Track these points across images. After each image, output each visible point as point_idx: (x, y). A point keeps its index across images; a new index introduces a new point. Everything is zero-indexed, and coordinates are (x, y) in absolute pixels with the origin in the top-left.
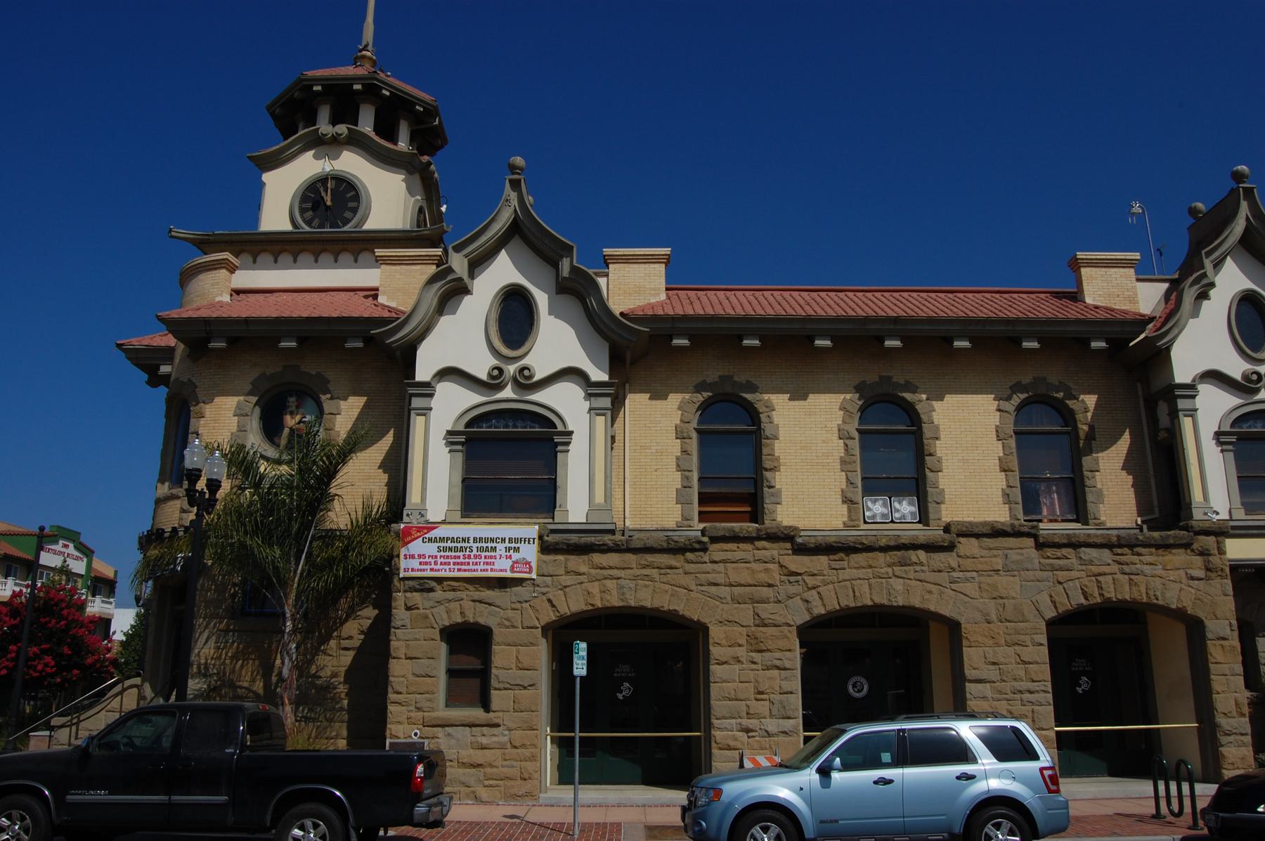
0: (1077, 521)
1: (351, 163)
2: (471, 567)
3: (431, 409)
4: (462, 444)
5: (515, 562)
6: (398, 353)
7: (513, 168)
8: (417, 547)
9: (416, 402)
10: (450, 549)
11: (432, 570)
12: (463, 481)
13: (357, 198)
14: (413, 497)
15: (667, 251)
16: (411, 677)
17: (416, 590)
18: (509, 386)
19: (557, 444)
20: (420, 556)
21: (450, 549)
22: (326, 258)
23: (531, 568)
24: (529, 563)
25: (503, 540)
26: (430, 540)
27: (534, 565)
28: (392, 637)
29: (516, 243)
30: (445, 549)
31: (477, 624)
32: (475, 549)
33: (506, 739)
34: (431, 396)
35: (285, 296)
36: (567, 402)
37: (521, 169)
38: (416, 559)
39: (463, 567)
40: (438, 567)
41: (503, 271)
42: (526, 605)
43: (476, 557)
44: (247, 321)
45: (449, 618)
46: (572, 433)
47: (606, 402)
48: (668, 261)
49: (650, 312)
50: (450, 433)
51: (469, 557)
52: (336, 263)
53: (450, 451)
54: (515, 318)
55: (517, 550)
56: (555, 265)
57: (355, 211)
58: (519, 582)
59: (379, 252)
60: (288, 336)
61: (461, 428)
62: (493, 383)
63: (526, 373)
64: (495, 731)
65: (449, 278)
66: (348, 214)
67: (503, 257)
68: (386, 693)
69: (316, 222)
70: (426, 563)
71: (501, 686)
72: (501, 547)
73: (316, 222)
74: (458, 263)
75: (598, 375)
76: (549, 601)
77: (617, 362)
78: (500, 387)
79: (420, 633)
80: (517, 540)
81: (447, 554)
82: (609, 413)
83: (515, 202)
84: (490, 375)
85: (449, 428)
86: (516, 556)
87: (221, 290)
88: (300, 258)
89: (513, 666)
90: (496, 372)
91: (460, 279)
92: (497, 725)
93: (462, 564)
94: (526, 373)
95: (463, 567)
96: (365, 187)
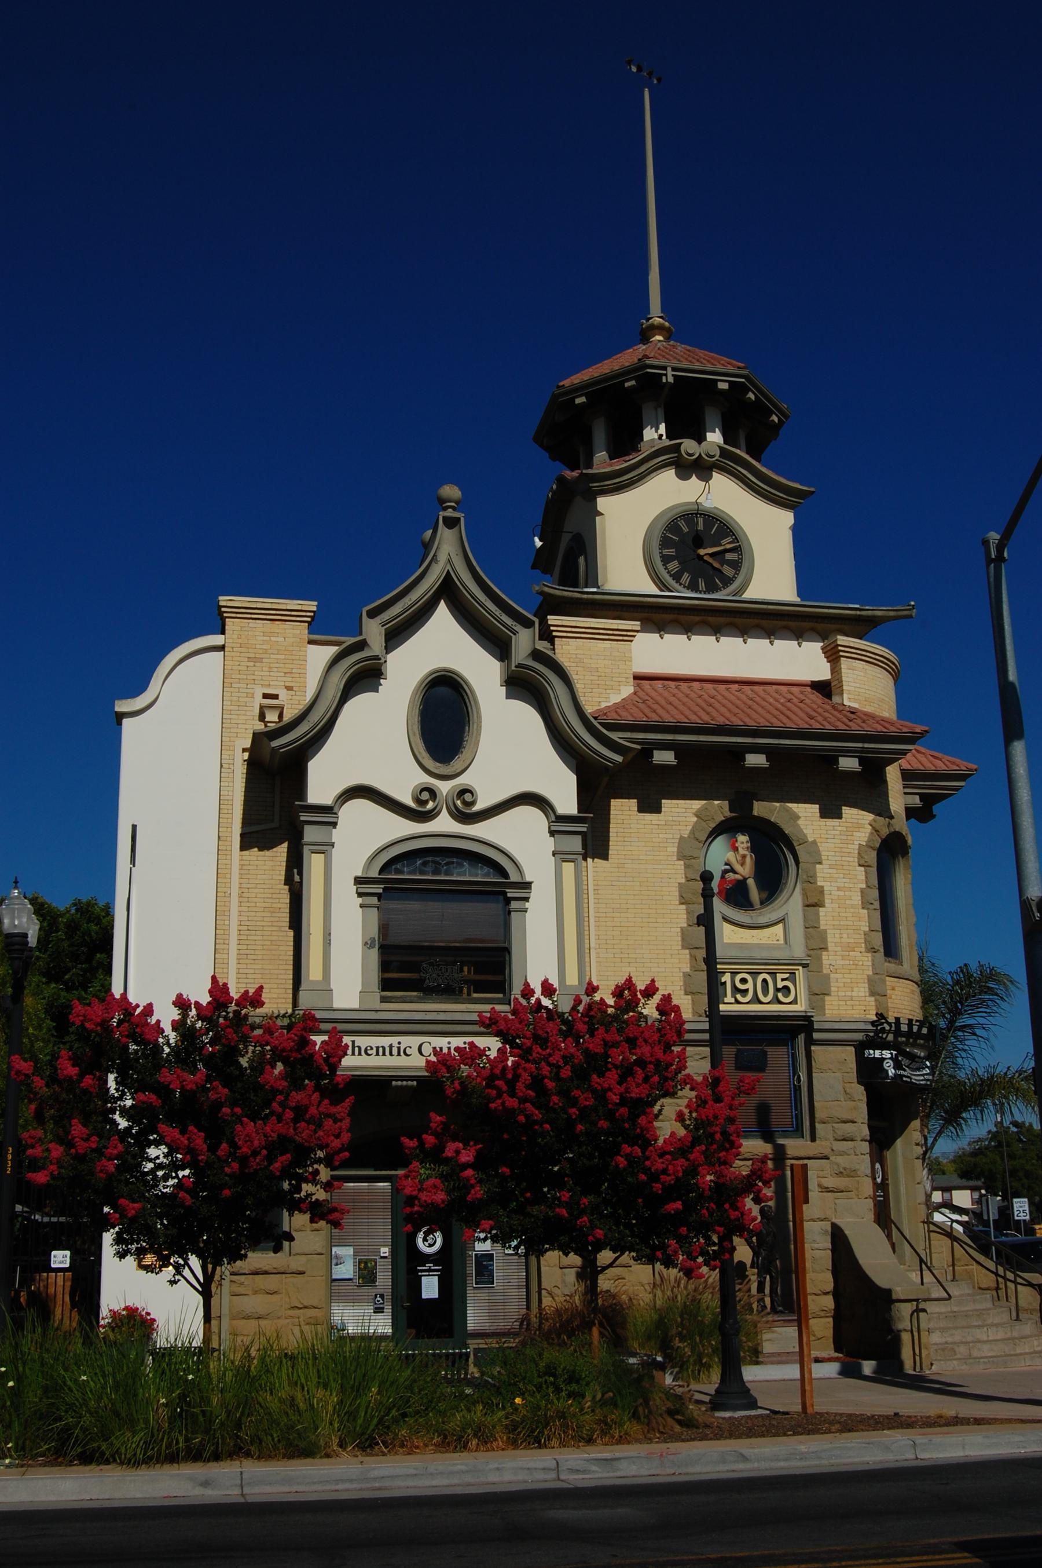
4: (379, 896)
9: (311, 834)
19: (508, 901)
36: (525, 842)
46: (530, 883)
47: (575, 844)
50: (358, 881)
54: (444, 718)
61: (374, 873)
63: (468, 797)
74: (374, 631)
77: (597, 786)
85: (360, 874)
90: (425, 796)
94: (468, 797)
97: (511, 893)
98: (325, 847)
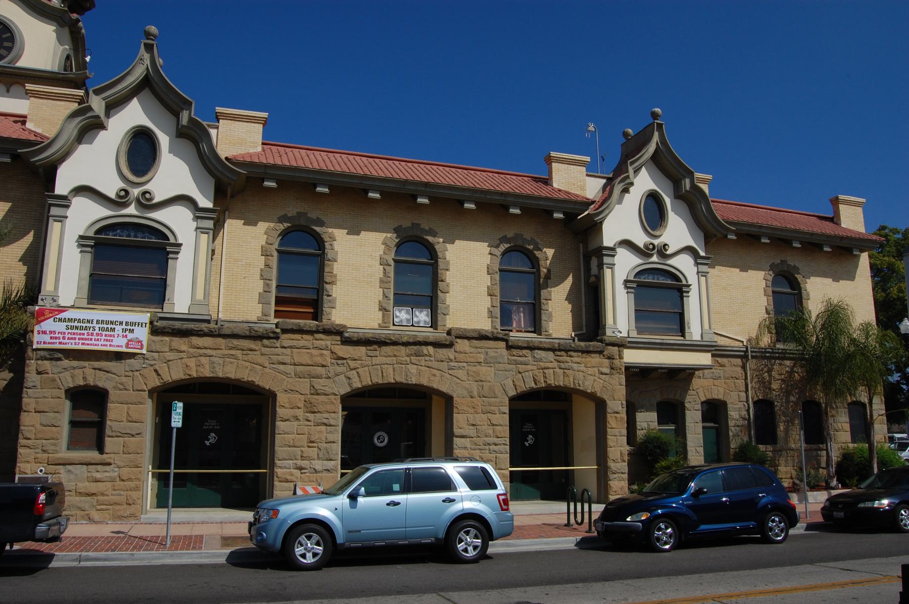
0: (534, 332)
2: (93, 342)
3: (66, 217)
5: (129, 341)
6: (41, 170)
7: (148, 35)
8: (48, 325)
9: (54, 211)
10: (77, 328)
11: (60, 343)
12: (91, 275)
13: (12, 39)
14: (48, 285)
15: (265, 115)
16: (38, 427)
17: (46, 359)
18: (133, 205)
19: (168, 253)
20: (51, 332)
21: (77, 328)
23: (142, 345)
24: (141, 342)
25: (121, 323)
26: (60, 320)
27: (145, 343)
28: (24, 395)
29: (146, 93)
30: (72, 328)
31: (96, 387)
32: (97, 329)
33: (116, 474)
34: (67, 207)
36: (179, 222)
37: (155, 36)
38: (46, 334)
39: (86, 342)
40: (66, 341)
41: (134, 115)
42: (137, 373)
43: (97, 334)
45: (73, 381)
46: (180, 245)
47: (210, 224)
48: (265, 123)
49: (249, 160)
50: (81, 237)
51: (92, 334)
53: (81, 252)
54: (141, 152)
55: (132, 331)
56: (177, 115)
57: (9, 50)
58: (132, 355)
59: (29, 86)
61: (91, 233)
62: (121, 201)
63: (147, 196)
64: (107, 468)
65: (89, 115)
67: (135, 104)
68: (17, 439)
70: (56, 338)
71: (114, 434)
72: (119, 328)
74: (97, 104)
75: (205, 202)
76: (156, 371)
77: (221, 193)
78: (125, 205)
79: (48, 392)
80: (132, 324)
81: (74, 331)
82: (211, 232)
83: (147, 62)
84: (118, 195)
85: (81, 234)
86: (130, 336)
89: (124, 419)
90: (123, 193)
91: (98, 117)
92: (110, 464)
93: (86, 339)
94: (147, 196)
95: (86, 342)
97: (169, 249)
98: (62, 219)
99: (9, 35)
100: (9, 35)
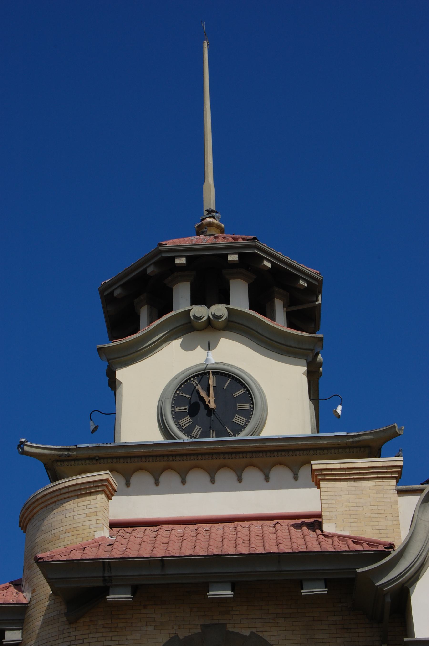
1: (232, 353)
6: (388, 599)
22: (225, 476)
35: (179, 529)
44: (163, 562)
52: (240, 482)
57: (248, 414)
59: (318, 464)
60: (220, 581)
66: (238, 419)
69: (197, 430)
73: (197, 430)
87: (91, 522)
88: (163, 478)
96: (255, 383)
99: (242, 391)
100: (242, 391)
